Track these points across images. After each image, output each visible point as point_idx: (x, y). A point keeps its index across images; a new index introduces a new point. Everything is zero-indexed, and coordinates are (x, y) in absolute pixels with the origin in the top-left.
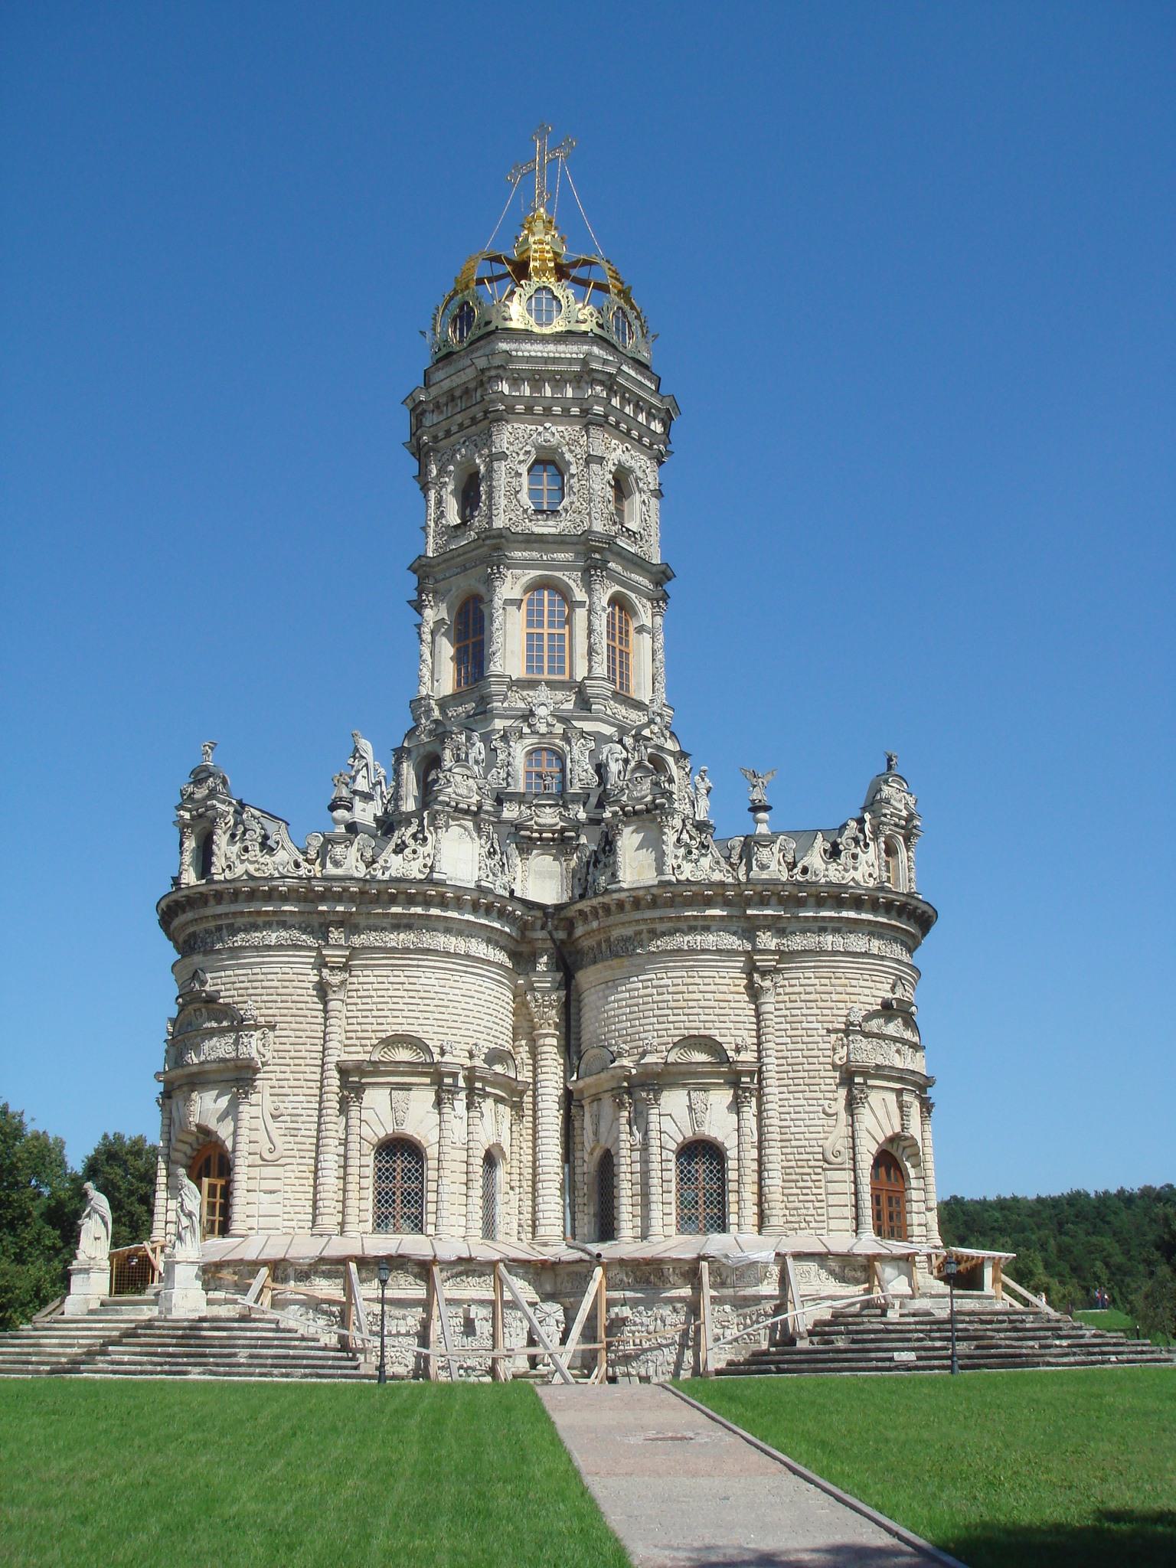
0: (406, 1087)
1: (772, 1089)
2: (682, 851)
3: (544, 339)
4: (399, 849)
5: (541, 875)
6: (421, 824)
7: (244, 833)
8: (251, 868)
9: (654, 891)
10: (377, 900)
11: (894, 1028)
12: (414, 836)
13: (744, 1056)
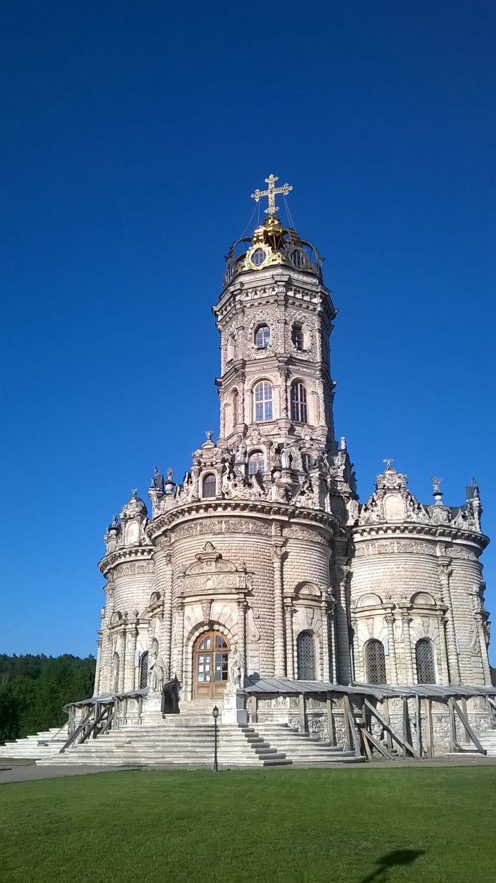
2: (411, 509)
3: (299, 272)
4: (303, 493)
6: (310, 484)
7: (235, 478)
8: (239, 494)
9: (405, 525)
10: (298, 516)
12: (307, 489)
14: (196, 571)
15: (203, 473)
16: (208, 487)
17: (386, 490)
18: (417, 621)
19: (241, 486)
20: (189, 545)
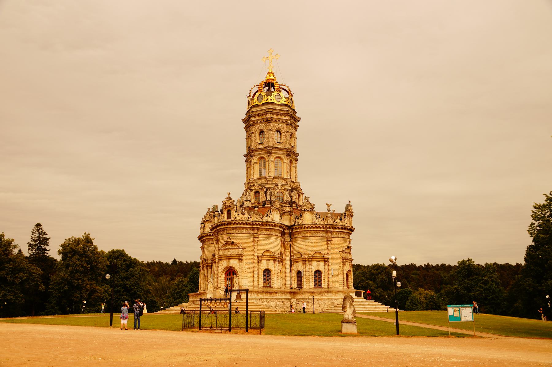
0: (269, 260)
1: (330, 261)
5: (286, 220)
10: (263, 225)
11: (348, 251)
13: (326, 256)
14: (225, 248)
15: (227, 209)
16: (229, 216)
17: (305, 210)
18: (314, 263)
19: (241, 215)
20: (223, 239)
